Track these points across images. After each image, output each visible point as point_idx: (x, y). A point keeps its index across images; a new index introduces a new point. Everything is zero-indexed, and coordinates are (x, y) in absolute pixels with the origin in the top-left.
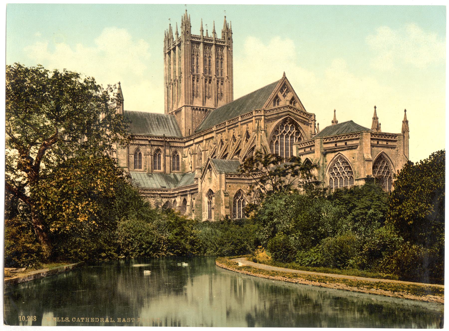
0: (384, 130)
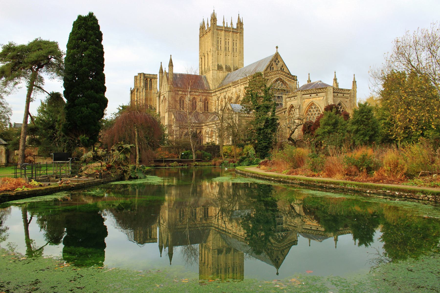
0: (340, 87)
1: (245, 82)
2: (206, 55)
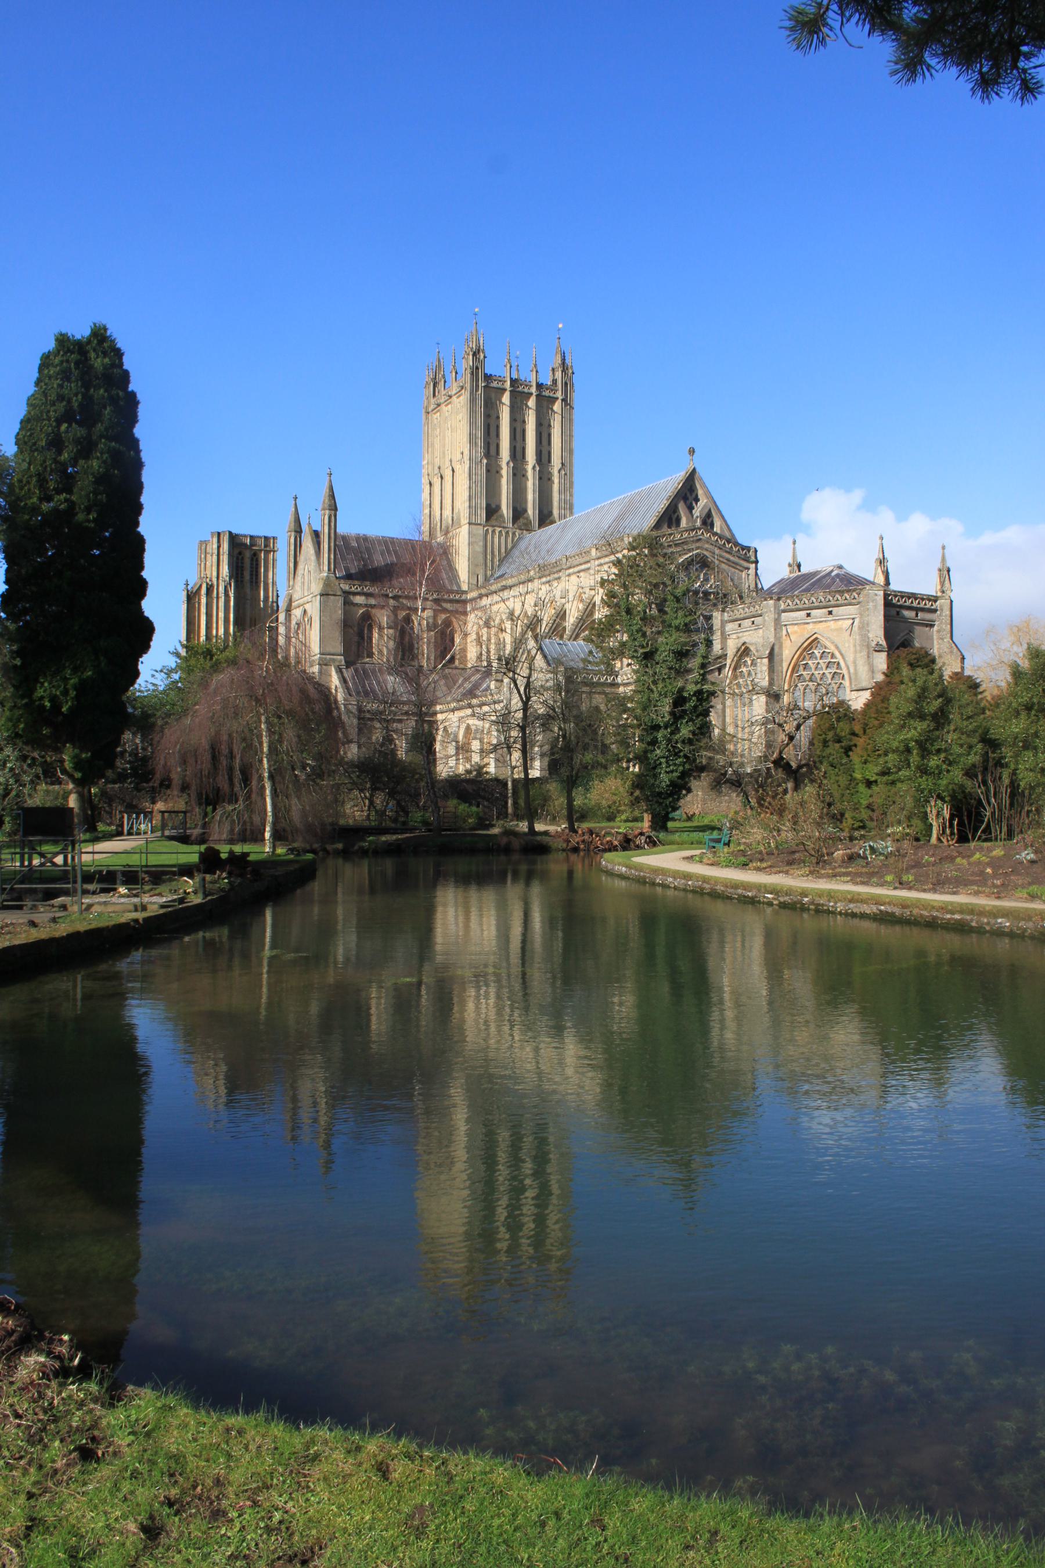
1: (583, 567)
2: (448, 474)
